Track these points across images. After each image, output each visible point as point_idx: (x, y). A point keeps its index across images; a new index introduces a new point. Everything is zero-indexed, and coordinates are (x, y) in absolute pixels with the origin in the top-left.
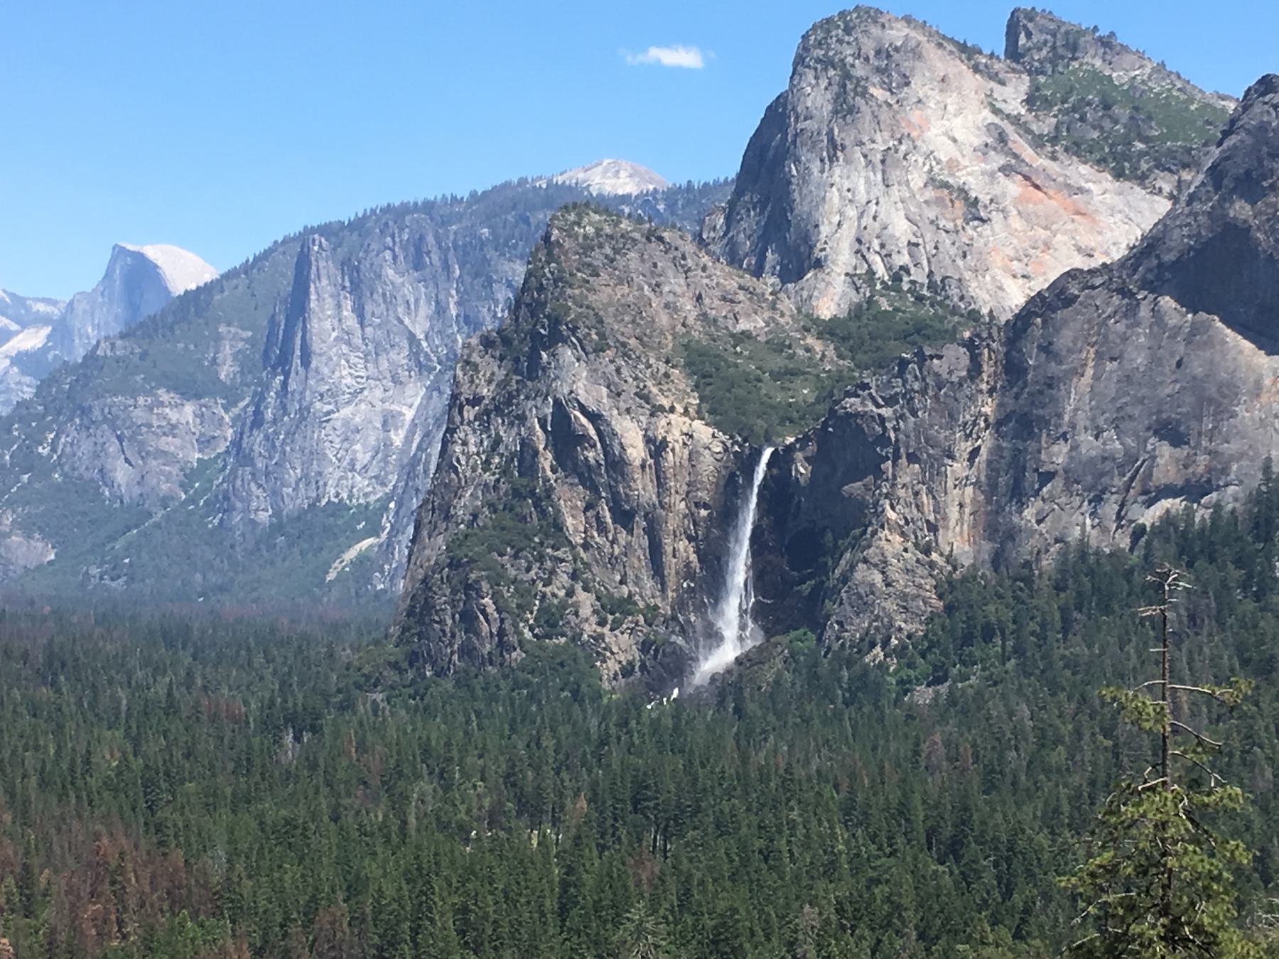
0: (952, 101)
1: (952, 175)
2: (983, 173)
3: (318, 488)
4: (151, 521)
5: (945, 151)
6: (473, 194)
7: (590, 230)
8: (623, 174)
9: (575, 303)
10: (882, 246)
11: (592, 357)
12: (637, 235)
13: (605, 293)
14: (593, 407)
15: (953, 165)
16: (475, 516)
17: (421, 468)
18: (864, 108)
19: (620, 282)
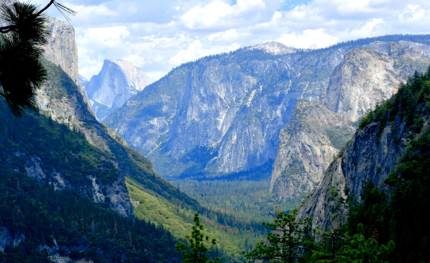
0: (377, 69)
1: (378, 87)
2: (385, 86)
3: (198, 143)
4: (149, 153)
5: (376, 81)
6: (231, 52)
7: (305, 106)
8: (275, 46)
9: (304, 123)
10: (364, 104)
11: (308, 134)
12: (314, 106)
13: (309, 120)
14: (309, 144)
15: (378, 85)
16: (286, 167)
17: (229, 137)
18: (359, 74)
19: (312, 117)
